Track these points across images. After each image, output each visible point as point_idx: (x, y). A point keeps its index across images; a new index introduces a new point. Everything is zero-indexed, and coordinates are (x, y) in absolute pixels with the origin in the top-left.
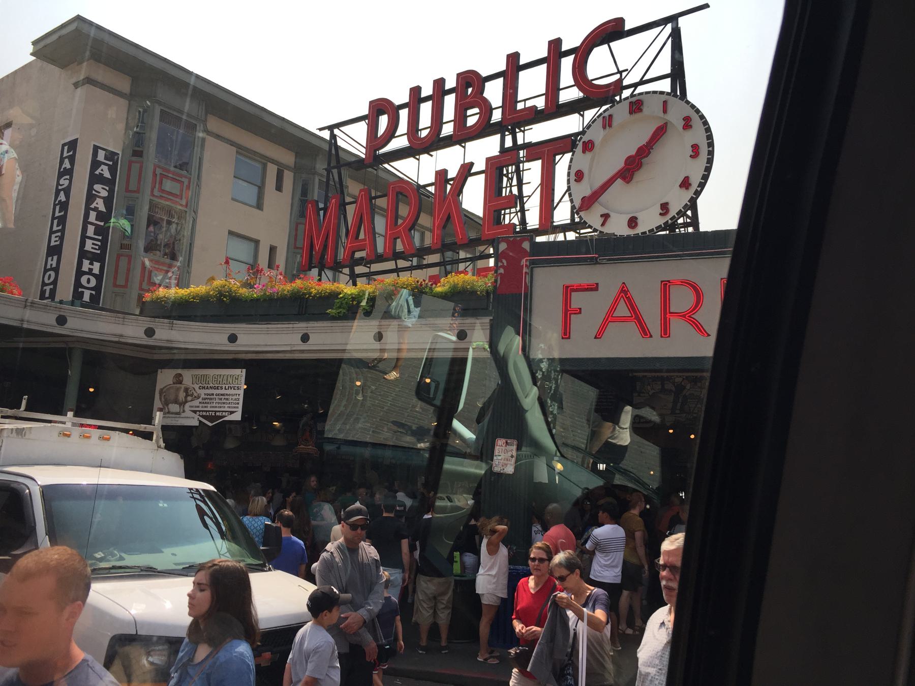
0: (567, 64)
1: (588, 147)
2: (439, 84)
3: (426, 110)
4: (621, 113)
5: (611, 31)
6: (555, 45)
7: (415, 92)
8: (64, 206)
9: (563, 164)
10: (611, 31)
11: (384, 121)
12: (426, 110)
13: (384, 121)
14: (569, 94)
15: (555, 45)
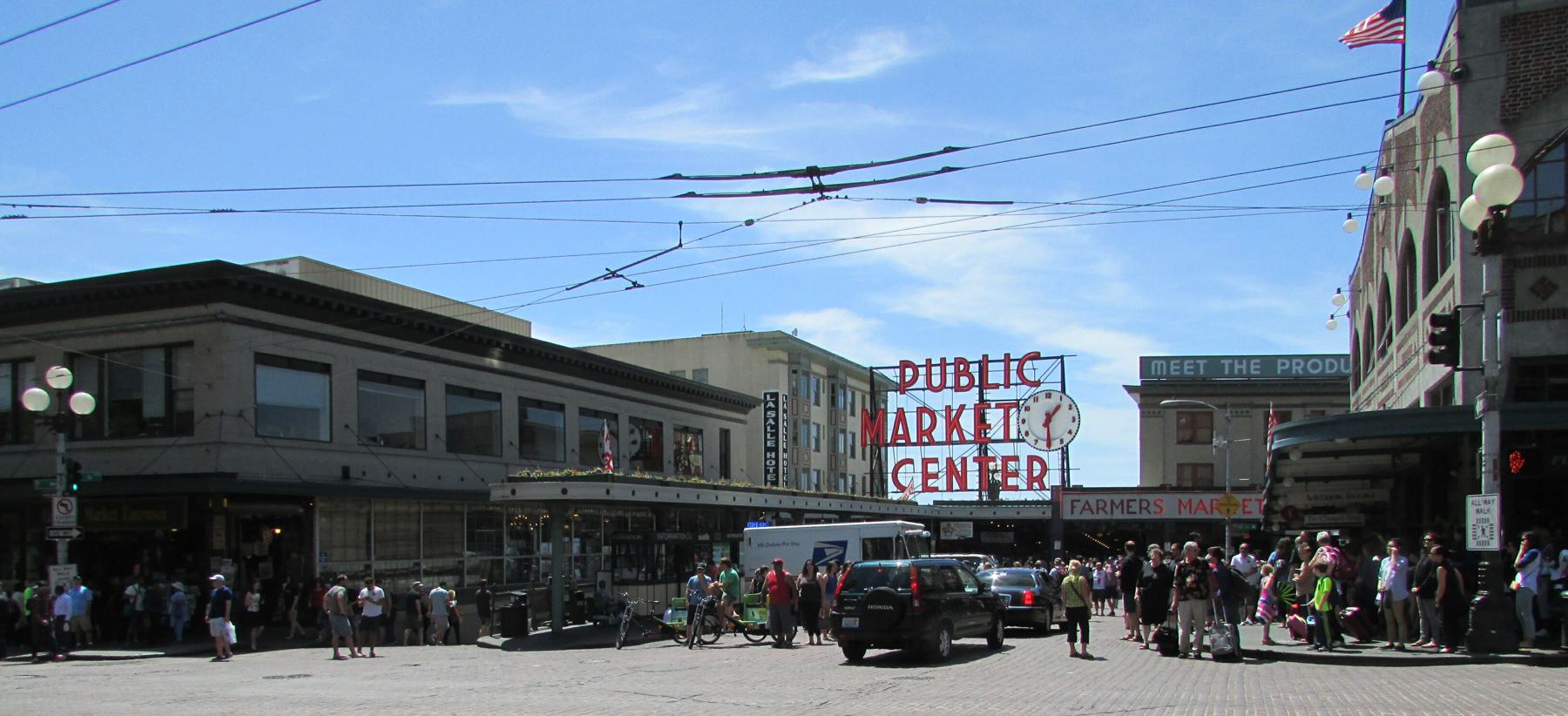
0: (1014, 365)
1: (1027, 409)
2: (943, 360)
3: (936, 370)
4: (1042, 397)
5: (1036, 356)
6: (1007, 355)
7: (929, 361)
8: (776, 427)
9: (1013, 411)
10: (1036, 356)
11: (909, 372)
12: (936, 370)
13: (909, 372)
14: (1014, 378)
15: (1007, 355)
